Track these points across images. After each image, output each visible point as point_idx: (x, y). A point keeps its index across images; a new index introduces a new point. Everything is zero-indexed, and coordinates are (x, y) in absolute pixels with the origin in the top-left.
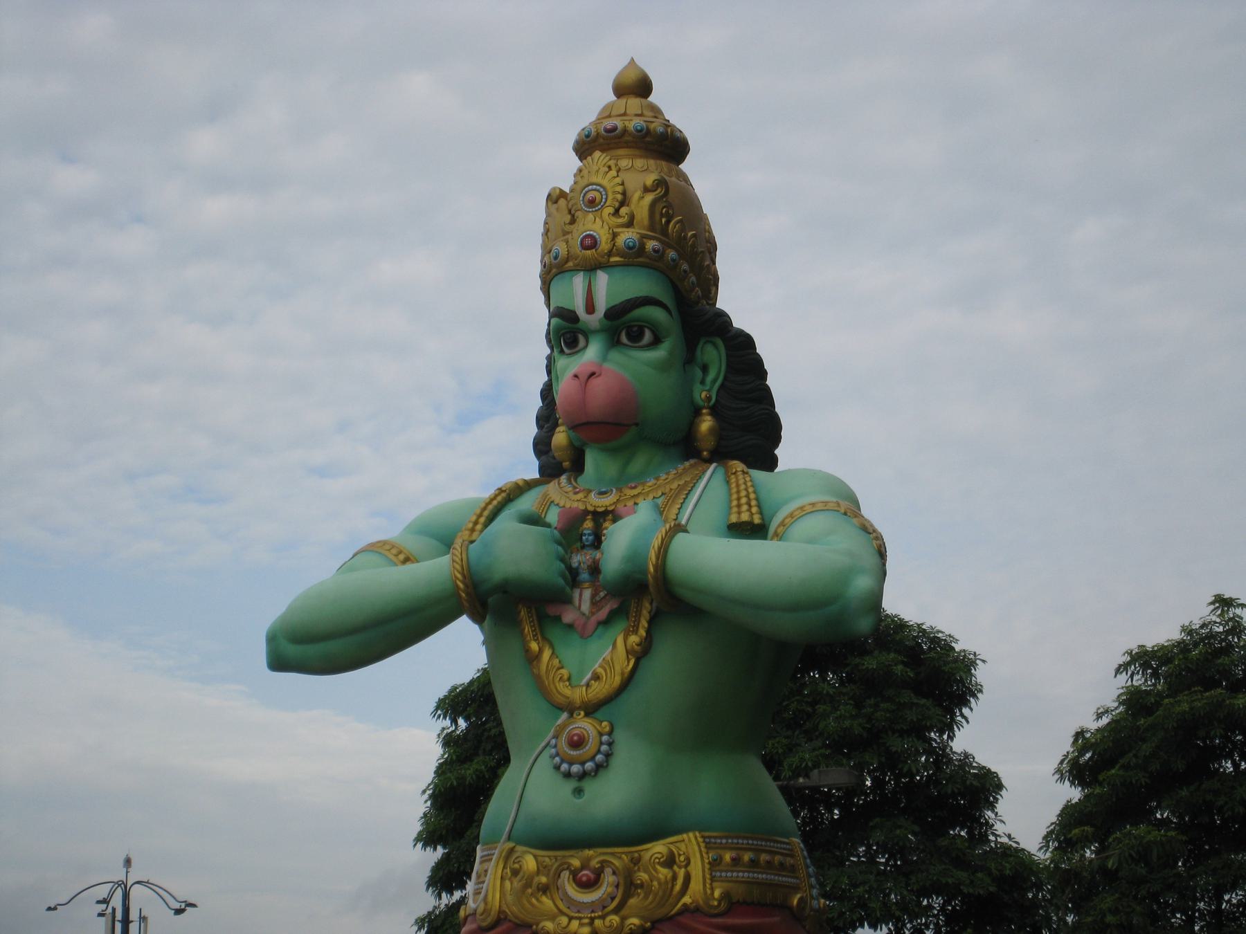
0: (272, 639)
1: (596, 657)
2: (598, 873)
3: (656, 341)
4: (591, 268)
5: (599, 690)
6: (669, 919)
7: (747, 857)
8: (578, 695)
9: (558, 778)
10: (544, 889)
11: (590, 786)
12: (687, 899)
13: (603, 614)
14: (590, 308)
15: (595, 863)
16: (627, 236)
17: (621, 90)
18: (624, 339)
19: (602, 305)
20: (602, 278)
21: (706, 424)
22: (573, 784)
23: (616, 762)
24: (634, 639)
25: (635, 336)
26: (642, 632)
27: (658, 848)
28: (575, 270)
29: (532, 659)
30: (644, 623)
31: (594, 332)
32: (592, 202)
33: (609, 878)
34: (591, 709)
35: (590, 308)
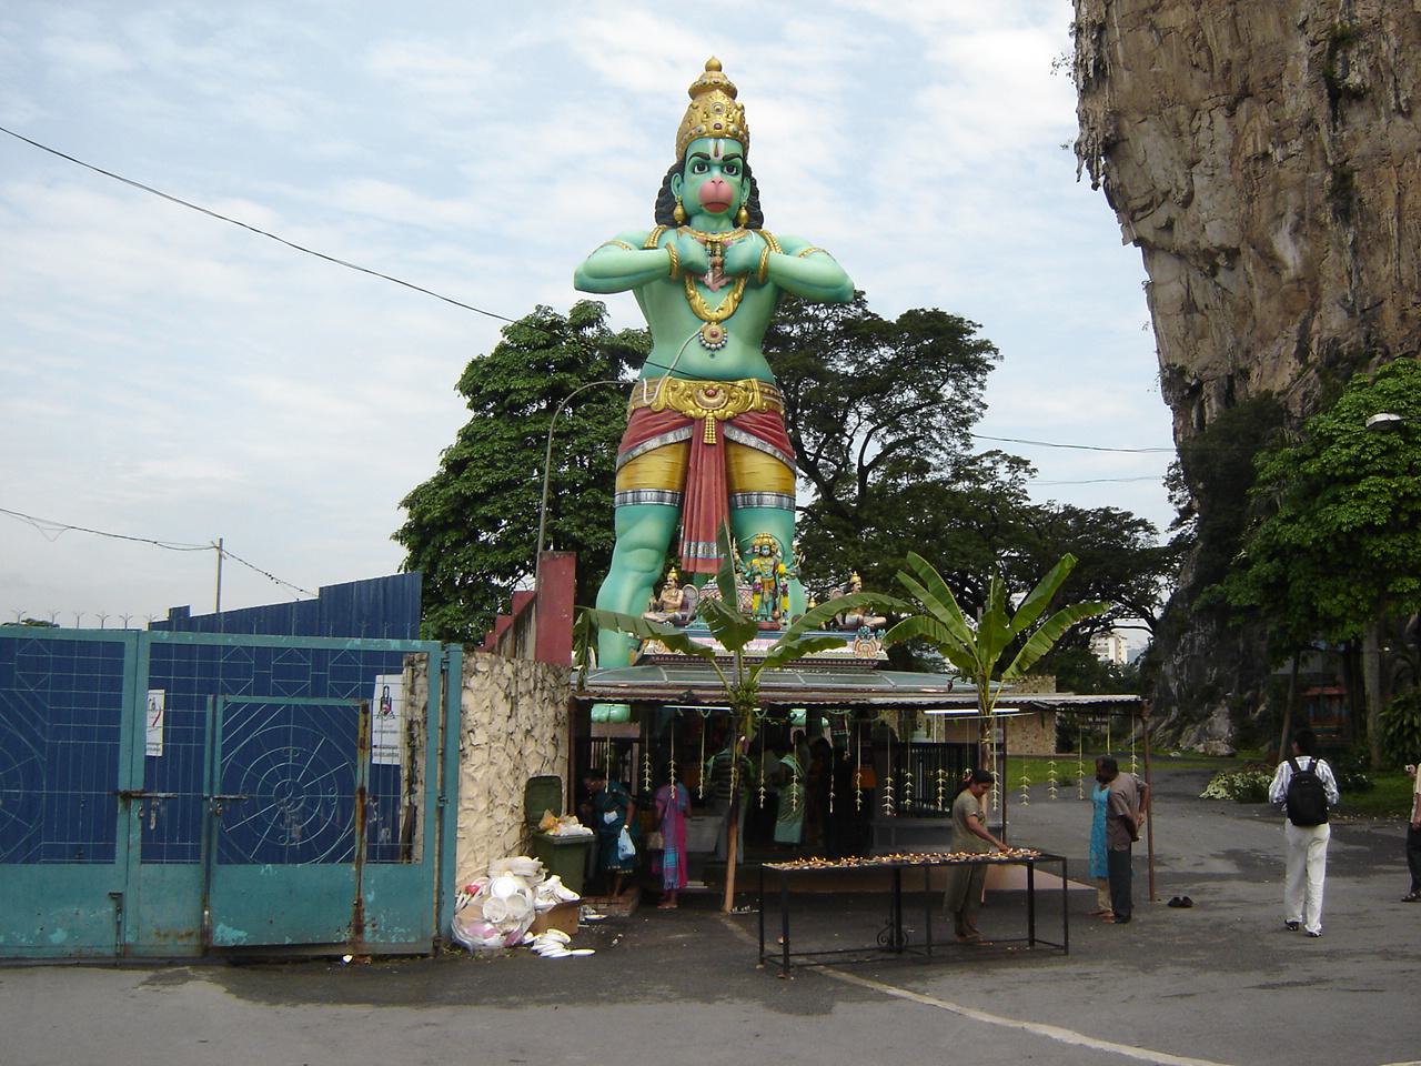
0: (577, 276)
1: (716, 302)
2: (716, 391)
3: (737, 174)
5: (722, 315)
6: (745, 413)
7: (766, 390)
8: (714, 315)
9: (703, 349)
10: (690, 397)
11: (716, 353)
12: (752, 405)
13: (723, 282)
14: (716, 155)
15: (715, 387)
16: (732, 127)
17: (709, 68)
19: (722, 154)
21: (744, 213)
22: (710, 352)
23: (728, 345)
24: (736, 296)
25: (730, 170)
26: (740, 292)
27: (740, 383)
28: (710, 138)
29: (689, 298)
30: (741, 288)
31: (715, 165)
32: (718, 110)
34: (719, 321)
35: (716, 155)
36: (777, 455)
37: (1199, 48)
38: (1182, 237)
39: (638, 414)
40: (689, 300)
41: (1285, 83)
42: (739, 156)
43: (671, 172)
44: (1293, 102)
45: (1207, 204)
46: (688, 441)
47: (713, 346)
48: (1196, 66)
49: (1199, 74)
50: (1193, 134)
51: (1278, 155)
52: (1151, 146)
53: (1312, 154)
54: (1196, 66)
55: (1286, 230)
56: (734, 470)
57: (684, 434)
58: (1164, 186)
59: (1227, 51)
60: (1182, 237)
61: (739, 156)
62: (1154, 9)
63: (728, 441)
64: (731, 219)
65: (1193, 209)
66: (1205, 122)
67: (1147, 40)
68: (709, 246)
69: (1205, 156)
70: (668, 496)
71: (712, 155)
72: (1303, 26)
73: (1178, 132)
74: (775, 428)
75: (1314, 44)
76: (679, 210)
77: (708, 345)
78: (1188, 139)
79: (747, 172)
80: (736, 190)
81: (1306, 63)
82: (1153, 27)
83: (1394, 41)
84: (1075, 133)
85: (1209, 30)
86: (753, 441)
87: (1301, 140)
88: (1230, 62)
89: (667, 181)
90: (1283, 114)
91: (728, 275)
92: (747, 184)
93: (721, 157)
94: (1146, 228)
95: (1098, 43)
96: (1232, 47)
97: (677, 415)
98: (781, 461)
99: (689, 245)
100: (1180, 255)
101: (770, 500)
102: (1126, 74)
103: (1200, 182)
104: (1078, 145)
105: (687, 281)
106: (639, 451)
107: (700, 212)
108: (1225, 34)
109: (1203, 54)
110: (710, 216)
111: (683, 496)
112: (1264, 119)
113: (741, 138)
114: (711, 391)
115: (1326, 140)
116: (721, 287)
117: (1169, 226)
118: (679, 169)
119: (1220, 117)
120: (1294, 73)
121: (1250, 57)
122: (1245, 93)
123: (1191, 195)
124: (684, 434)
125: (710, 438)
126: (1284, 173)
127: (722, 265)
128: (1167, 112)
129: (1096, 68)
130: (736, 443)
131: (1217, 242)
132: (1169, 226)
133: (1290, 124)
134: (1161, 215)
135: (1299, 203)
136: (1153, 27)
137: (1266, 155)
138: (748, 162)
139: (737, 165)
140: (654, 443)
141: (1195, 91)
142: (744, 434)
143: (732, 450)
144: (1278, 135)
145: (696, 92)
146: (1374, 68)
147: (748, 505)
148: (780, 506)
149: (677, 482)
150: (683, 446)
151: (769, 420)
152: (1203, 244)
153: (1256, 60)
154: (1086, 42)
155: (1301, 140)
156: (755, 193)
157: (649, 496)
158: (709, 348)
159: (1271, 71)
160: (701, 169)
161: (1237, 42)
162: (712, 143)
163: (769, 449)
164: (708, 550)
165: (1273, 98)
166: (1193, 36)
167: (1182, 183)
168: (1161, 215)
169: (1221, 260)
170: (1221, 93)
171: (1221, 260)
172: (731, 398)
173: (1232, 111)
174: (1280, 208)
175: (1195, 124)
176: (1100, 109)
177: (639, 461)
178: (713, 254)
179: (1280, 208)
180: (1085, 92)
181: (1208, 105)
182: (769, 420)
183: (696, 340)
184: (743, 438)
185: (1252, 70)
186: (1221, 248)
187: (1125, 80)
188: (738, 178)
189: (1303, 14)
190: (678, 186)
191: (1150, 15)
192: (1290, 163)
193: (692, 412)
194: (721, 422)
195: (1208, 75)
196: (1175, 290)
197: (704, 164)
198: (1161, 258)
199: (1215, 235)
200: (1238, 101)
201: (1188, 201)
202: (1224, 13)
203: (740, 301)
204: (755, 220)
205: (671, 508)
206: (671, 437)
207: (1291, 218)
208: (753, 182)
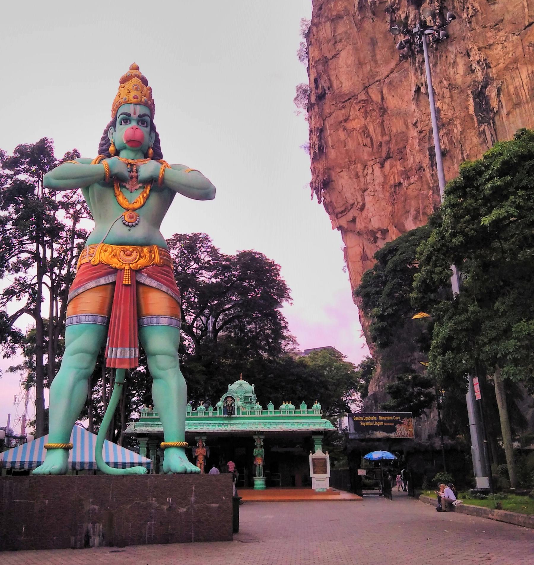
2: (132, 252)
3: (147, 127)
4: (135, 104)
5: (136, 206)
9: (124, 226)
11: (132, 229)
14: (135, 113)
15: (131, 250)
18: (140, 123)
20: (138, 108)
22: (128, 228)
23: (141, 224)
26: (148, 192)
31: (133, 120)
33: (134, 254)
34: (134, 210)
35: (135, 113)
36: (169, 292)
37: (367, 137)
38: (360, 225)
39: (82, 267)
40: (116, 196)
41: (408, 150)
42: (148, 116)
43: (109, 127)
44: (412, 159)
45: (372, 209)
46: (113, 284)
47: (130, 224)
48: (365, 145)
49: (367, 149)
50: (365, 177)
51: (405, 183)
52: (345, 182)
53: (422, 182)
54: (365, 145)
55: (411, 218)
56: (142, 301)
57: (111, 279)
58: (351, 202)
59: (380, 138)
60: (360, 225)
61: (148, 116)
62: (346, 121)
63: (138, 284)
64: (143, 152)
65: (365, 213)
66: (370, 171)
67: (342, 135)
68: (129, 166)
69: (370, 187)
70: (100, 319)
71: (132, 114)
72: (415, 125)
73: (357, 176)
74: (167, 275)
75: (421, 132)
76: (112, 148)
77: (127, 223)
78: (362, 179)
79: (153, 128)
80: (147, 136)
81: (418, 141)
82: (345, 129)
83: (460, 128)
84: (309, 177)
85: (371, 129)
86: (154, 284)
87: (417, 176)
88: (381, 143)
89: (106, 132)
90: (407, 165)
91: (141, 182)
92: (153, 135)
93: (137, 114)
94: (343, 222)
95: (320, 138)
96: (382, 136)
97: (106, 267)
98: (172, 296)
99: (118, 164)
100: (359, 234)
101: (164, 321)
102: (332, 151)
103: (368, 199)
104: (311, 183)
105: (115, 185)
106: (82, 290)
107: (124, 148)
108: (379, 130)
109: (369, 140)
110: (130, 150)
111: (109, 319)
112: (399, 167)
113: (150, 106)
114: (128, 252)
115: (428, 175)
116: (136, 190)
117: (354, 220)
118: (113, 124)
119: (377, 168)
120: (412, 146)
121: (391, 140)
122: (388, 157)
123: (364, 205)
124: (111, 279)
125: (126, 281)
126: (409, 192)
127: (137, 177)
128: (352, 167)
129: (319, 148)
130: (144, 285)
131: (376, 227)
132: (354, 220)
133: (411, 169)
134: (350, 216)
135: (417, 205)
136: (345, 129)
137: (400, 184)
138: (154, 121)
139: (147, 120)
140: (92, 284)
141: (365, 157)
142: (148, 279)
143: (141, 289)
144: (406, 174)
145: (124, 80)
146: (451, 142)
147: (150, 324)
148: (170, 325)
149: (106, 309)
150: (110, 287)
151: (164, 270)
152: (370, 228)
153: (394, 141)
154: (314, 137)
155: (417, 176)
156: (157, 141)
157: (87, 319)
158: (128, 226)
159: (401, 146)
160: (126, 122)
161: (383, 134)
162: (132, 106)
163: (164, 288)
164: (124, 353)
165: (403, 158)
166: (364, 131)
167: (360, 199)
168: (350, 216)
169: (379, 235)
170: (377, 157)
171: (379, 235)
172: (141, 257)
173: (382, 166)
174: (407, 208)
175: (365, 172)
176: (321, 167)
177: (82, 296)
178: (131, 171)
179: (407, 208)
180: (315, 159)
181: (372, 163)
182: (164, 270)
183: (120, 220)
184: (148, 281)
185: (391, 146)
186: (379, 229)
187: (332, 153)
188: (148, 129)
189: (415, 119)
190: (112, 134)
191: (343, 124)
192: (411, 186)
193: (117, 266)
194: (137, 272)
195: (371, 149)
196: (356, 251)
197: (127, 120)
198: (350, 235)
199: (375, 224)
200: (385, 161)
201: (362, 209)
202: (378, 121)
203: (148, 198)
204: (158, 156)
205: (102, 327)
206: (102, 281)
207: (413, 212)
208: (157, 135)
